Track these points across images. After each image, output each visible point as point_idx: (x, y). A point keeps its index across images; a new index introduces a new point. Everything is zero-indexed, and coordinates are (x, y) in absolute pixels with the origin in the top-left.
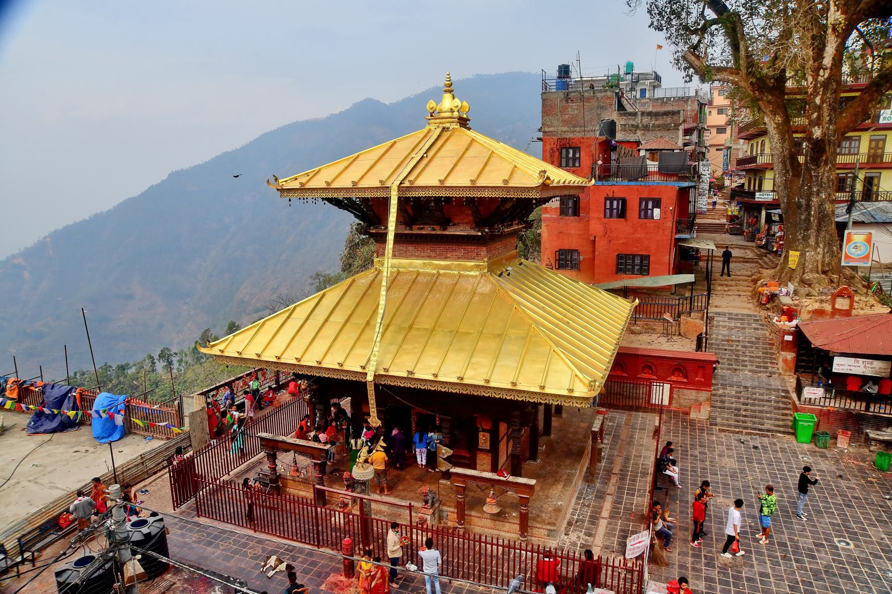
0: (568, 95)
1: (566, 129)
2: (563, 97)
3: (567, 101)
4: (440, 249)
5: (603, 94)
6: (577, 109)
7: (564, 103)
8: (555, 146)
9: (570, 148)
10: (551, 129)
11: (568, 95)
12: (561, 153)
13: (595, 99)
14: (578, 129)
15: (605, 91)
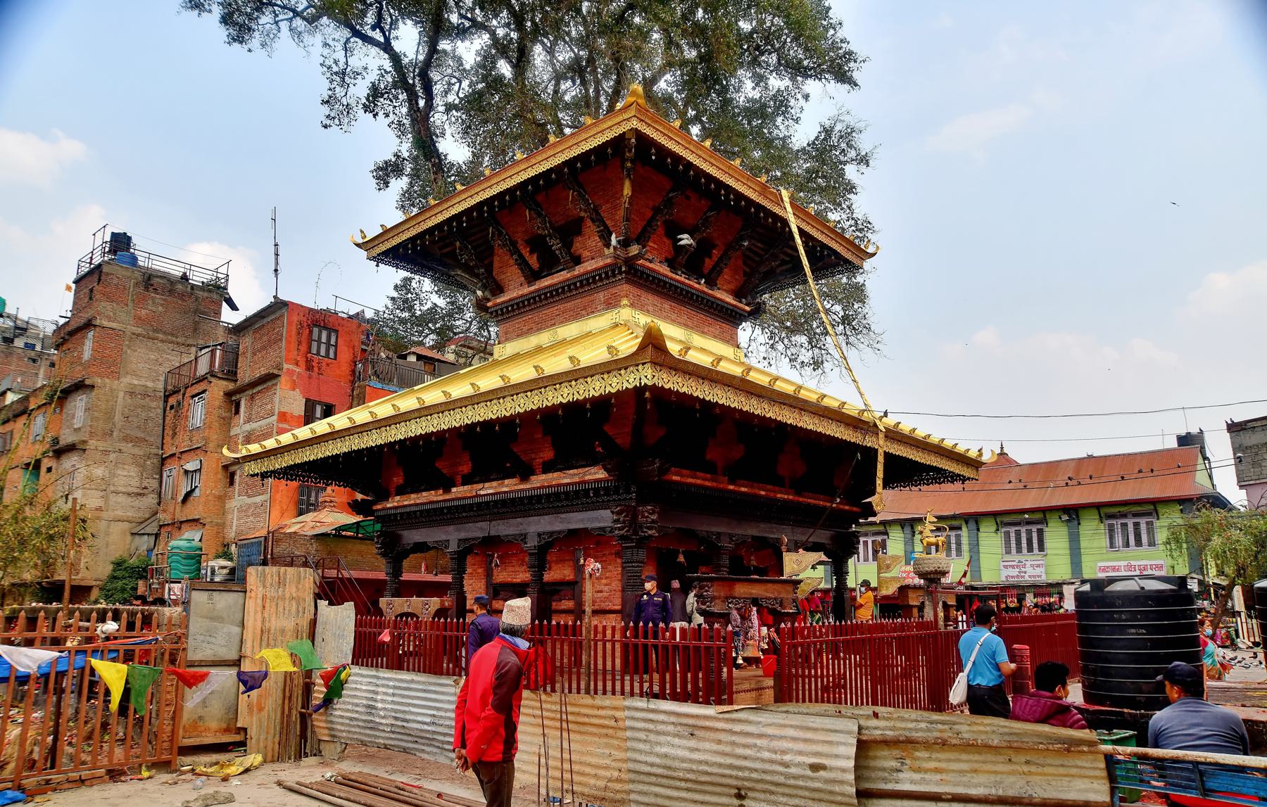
0: (149, 279)
1: (139, 330)
2: (140, 279)
3: (147, 288)
4: (699, 317)
5: (206, 294)
6: (162, 305)
7: (141, 289)
8: (305, 319)
9: (325, 328)
10: (114, 325)
11: (149, 279)
12: (311, 332)
13: (194, 299)
14: (161, 336)
15: (210, 291)
